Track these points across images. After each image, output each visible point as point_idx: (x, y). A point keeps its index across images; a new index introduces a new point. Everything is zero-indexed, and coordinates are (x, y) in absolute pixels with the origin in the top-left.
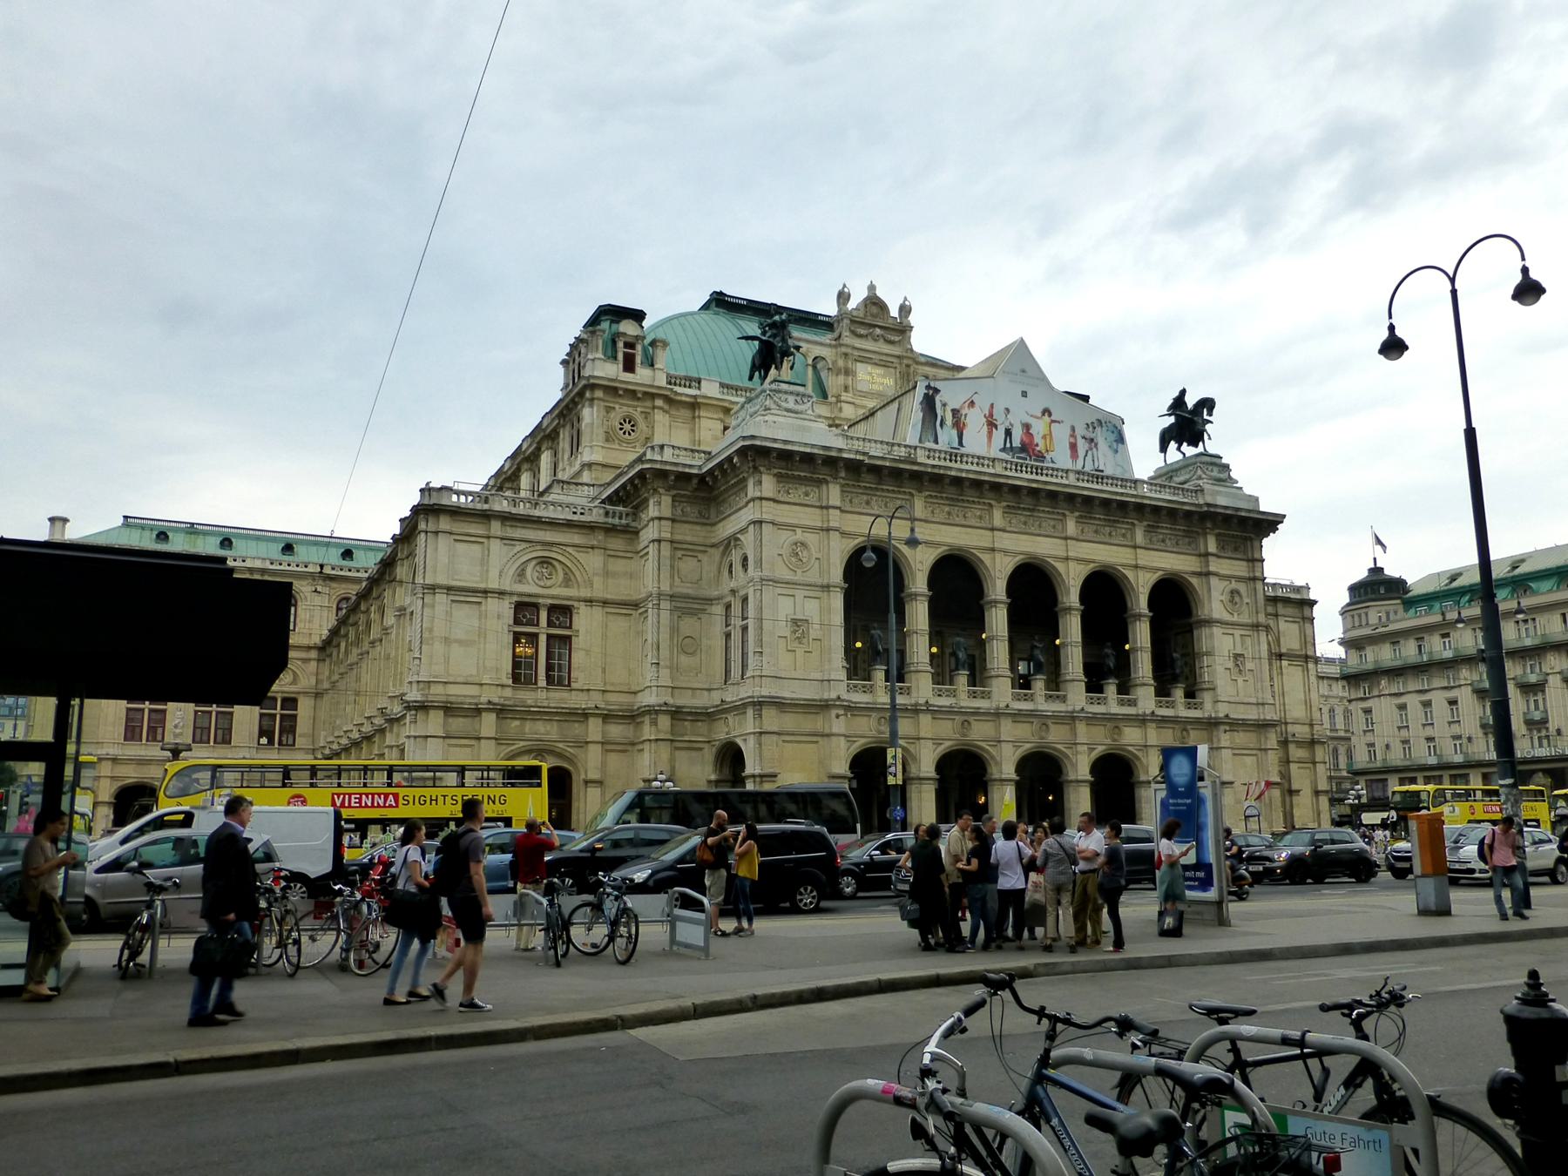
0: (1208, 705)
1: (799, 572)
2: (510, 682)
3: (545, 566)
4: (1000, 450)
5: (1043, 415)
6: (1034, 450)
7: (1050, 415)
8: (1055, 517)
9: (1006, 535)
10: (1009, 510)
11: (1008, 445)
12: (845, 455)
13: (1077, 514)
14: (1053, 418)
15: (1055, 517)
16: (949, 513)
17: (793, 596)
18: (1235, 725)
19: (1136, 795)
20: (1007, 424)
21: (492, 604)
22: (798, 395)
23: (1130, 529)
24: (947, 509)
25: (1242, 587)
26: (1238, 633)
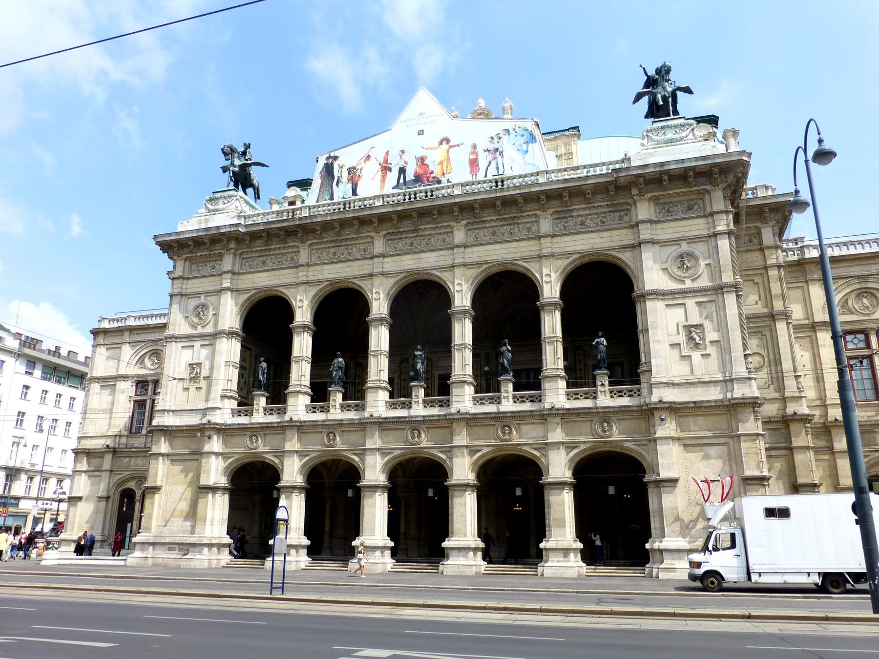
0: (644, 391)
1: (199, 327)
2: (126, 433)
3: (155, 355)
4: (393, 188)
5: (441, 143)
6: (428, 178)
7: (448, 141)
8: (443, 231)
9: (387, 260)
10: (390, 237)
11: (402, 181)
12: (222, 231)
13: (464, 222)
14: (451, 144)
15: (443, 231)
16: (335, 254)
17: (193, 346)
18: (675, 409)
19: (546, 498)
20: (402, 164)
21: (121, 385)
22: (225, 198)
23: (536, 221)
24: (333, 250)
25: (699, 249)
26: (691, 303)
